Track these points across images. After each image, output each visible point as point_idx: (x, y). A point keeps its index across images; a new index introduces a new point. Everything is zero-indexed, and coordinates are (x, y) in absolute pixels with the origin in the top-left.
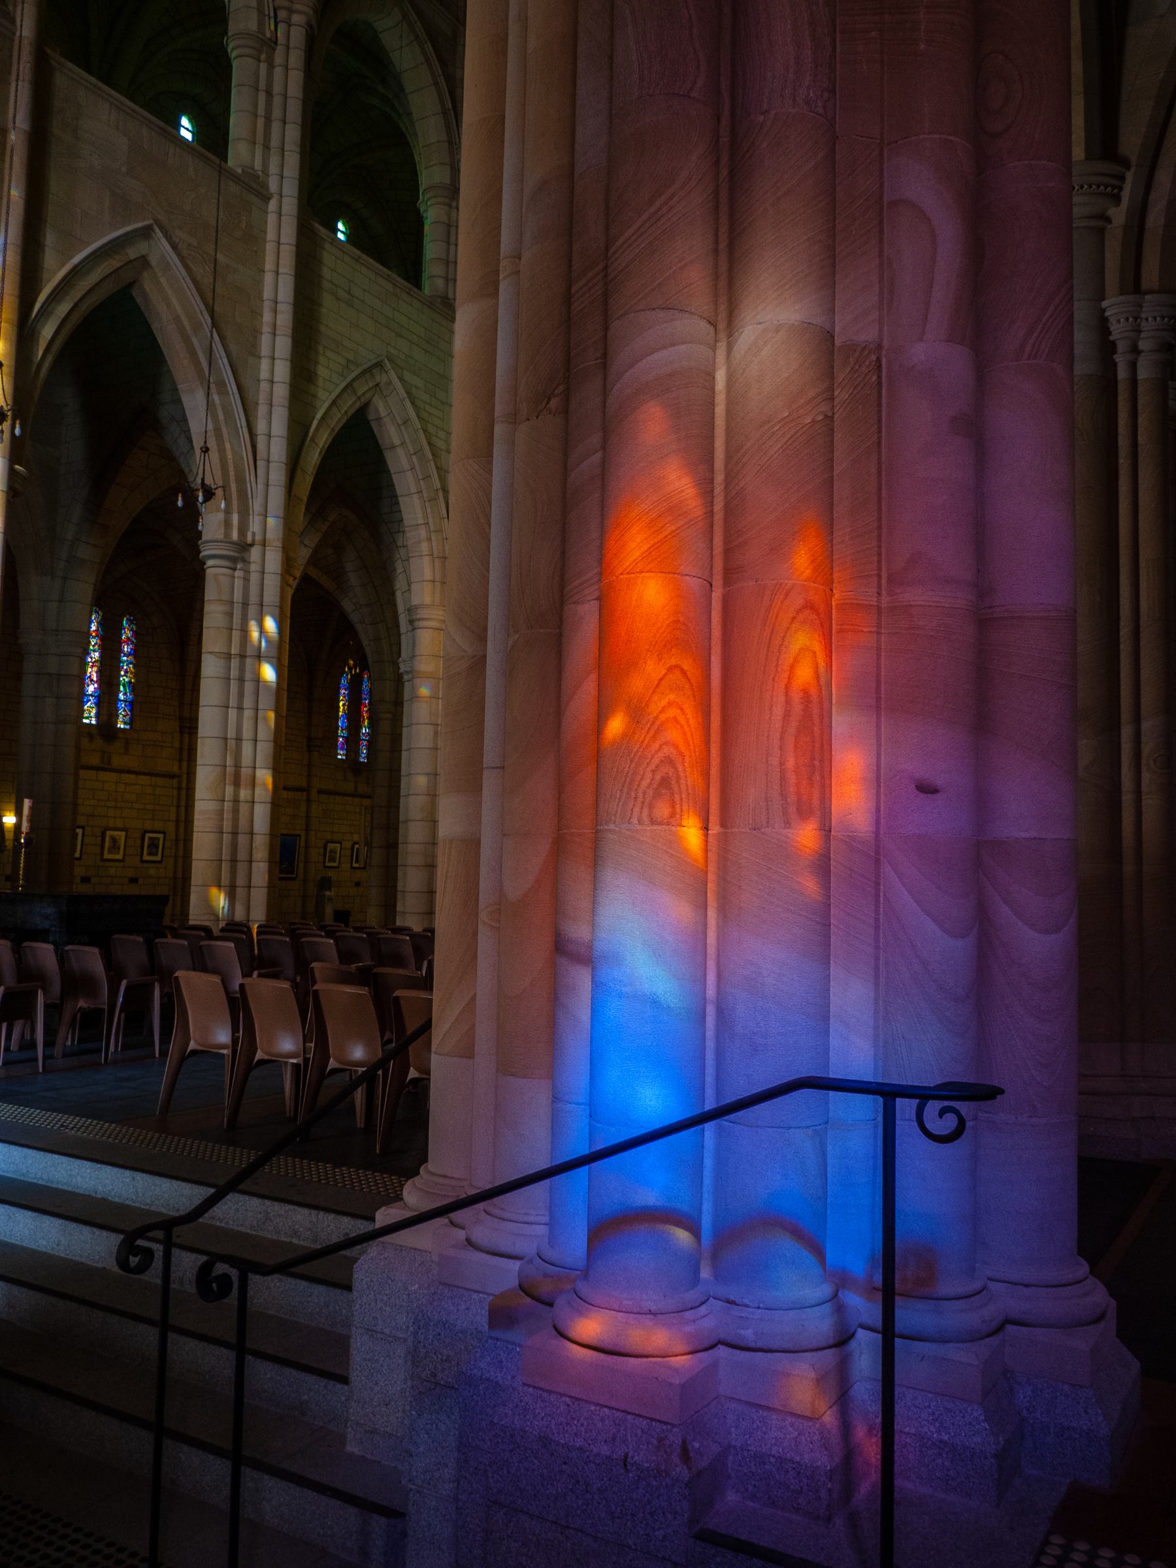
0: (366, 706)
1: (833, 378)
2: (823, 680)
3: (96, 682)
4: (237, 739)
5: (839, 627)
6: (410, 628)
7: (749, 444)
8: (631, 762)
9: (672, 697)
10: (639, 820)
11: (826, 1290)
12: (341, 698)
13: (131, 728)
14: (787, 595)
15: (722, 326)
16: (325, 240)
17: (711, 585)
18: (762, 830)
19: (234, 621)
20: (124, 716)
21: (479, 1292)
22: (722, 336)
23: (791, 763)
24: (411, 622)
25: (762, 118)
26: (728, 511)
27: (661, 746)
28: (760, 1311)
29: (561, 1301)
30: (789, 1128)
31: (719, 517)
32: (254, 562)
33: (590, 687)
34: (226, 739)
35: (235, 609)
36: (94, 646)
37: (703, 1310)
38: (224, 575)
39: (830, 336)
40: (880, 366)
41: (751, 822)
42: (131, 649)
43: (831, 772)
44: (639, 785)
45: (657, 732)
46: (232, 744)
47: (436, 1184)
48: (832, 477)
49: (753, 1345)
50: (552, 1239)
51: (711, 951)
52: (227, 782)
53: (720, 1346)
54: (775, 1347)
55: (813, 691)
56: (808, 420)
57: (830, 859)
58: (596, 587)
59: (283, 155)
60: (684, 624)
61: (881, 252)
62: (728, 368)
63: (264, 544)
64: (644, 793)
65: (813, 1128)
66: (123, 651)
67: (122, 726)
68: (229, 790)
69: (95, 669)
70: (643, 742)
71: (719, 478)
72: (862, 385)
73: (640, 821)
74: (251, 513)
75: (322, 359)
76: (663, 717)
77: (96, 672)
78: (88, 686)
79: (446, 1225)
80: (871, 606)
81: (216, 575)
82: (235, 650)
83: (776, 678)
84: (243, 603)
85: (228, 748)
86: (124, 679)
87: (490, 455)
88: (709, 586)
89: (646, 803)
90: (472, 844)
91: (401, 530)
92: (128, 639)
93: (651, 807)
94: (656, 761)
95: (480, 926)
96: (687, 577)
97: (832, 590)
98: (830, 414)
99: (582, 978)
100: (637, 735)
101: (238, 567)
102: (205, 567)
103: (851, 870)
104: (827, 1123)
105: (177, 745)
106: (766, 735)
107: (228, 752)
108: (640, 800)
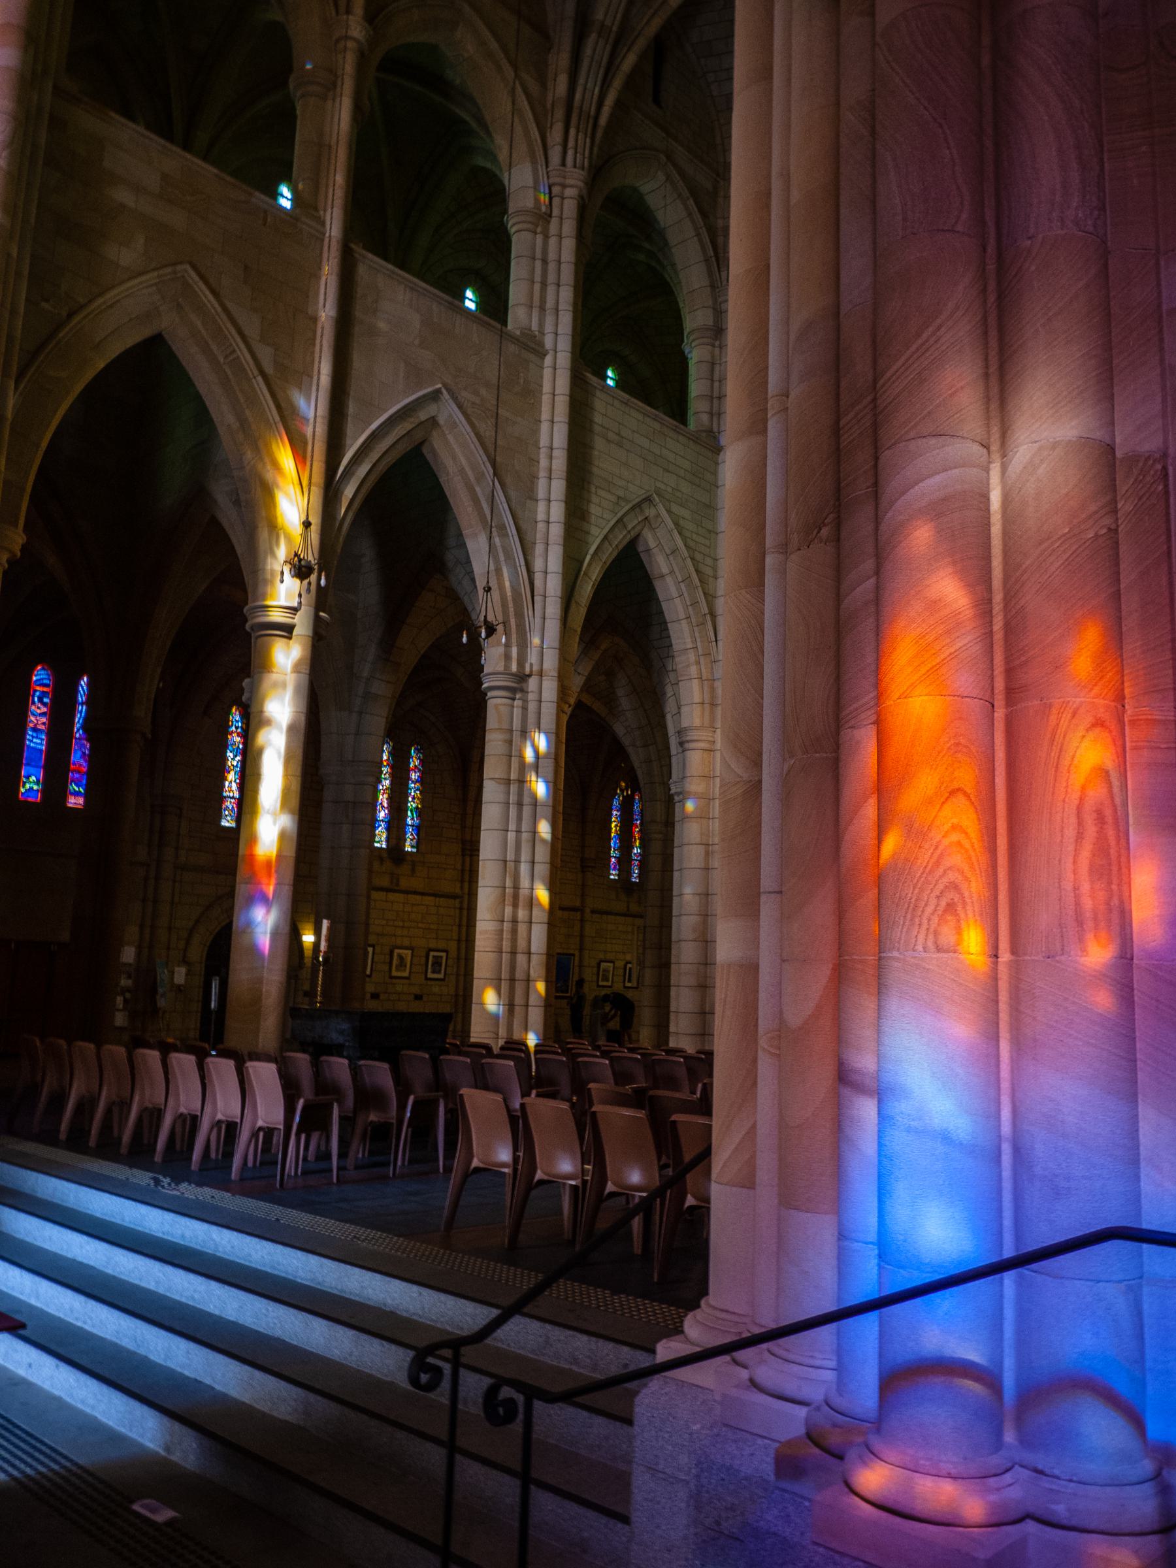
0: (637, 827)
1: (1115, 491)
2: (1118, 800)
4: (515, 861)
5: (1134, 744)
6: (680, 750)
7: (1028, 562)
8: (914, 888)
9: (955, 821)
10: (924, 948)
11: (1147, 1466)
12: (613, 819)
13: (417, 851)
14: (1074, 714)
15: (995, 447)
16: (596, 387)
17: (993, 706)
18: (1057, 958)
20: (411, 840)
21: (765, 1438)
22: (996, 456)
23: (1086, 887)
24: (681, 744)
25: (1029, 242)
26: (1008, 629)
27: (945, 871)
28: (1072, 1485)
29: (852, 1454)
30: (1099, 1282)
31: (998, 636)
32: (532, 692)
33: (870, 810)
34: (505, 861)
37: (1008, 1478)
39: (1111, 448)
40: (1166, 475)
41: (1044, 949)
43: (1130, 896)
44: (923, 911)
45: (941, 856)
46: (511, 865)
47: (718, 1318)
48: (1119, 590)
49: (1065, 1522)
50: (841, 1384)
51: (1005, 1085)
52: (506, 903)
53: (1028, 1521)
54: (1093, 1526)
55: (1108, 812)
56: (1091, 535)
57: (1132, 989)
58: (873, 711)
59: (557, 315)
60: (967, 747)
61: (1162, 360)
62: (1003, 488)
63: (541, 674)
64: (929, 920)
65: (1125, 1283)
66: (411, 779)
67: (410, 850)
68: (508, 910)
69: (386, 796)
70: (926, 867)
71: (998, 597)
72: (1147, 495)
73: (925, 949)
74: (529, 646)
75: (594, 499)
76: (946, 842)
77: (387, 799)
78: (380, 812)
79: (728, 1363)
80: (1168, 721)
81: (496, 706)
82: (513, 776)
83: (1067, 800)
86: (412, 805)
87: (762, 584)
88: (990, 705)
89: (931, 930)
90: (750, 969)
91: (670, 654)
92: (416, 766)
93: (936, 933)
94: (941, 886)
95: (760, 1053)
96: (967, 699)
97: (1123, 706)
98: (1113, 527)
99: (866, 1109)
100: (919, 861)
101: (517, 696)
102: (487, 698)
103: (1157, 1001)
104: (1141, 1277)
105: (459, 867)
106: (1057, 859)
107: (508, 875)
108: (925, 926)
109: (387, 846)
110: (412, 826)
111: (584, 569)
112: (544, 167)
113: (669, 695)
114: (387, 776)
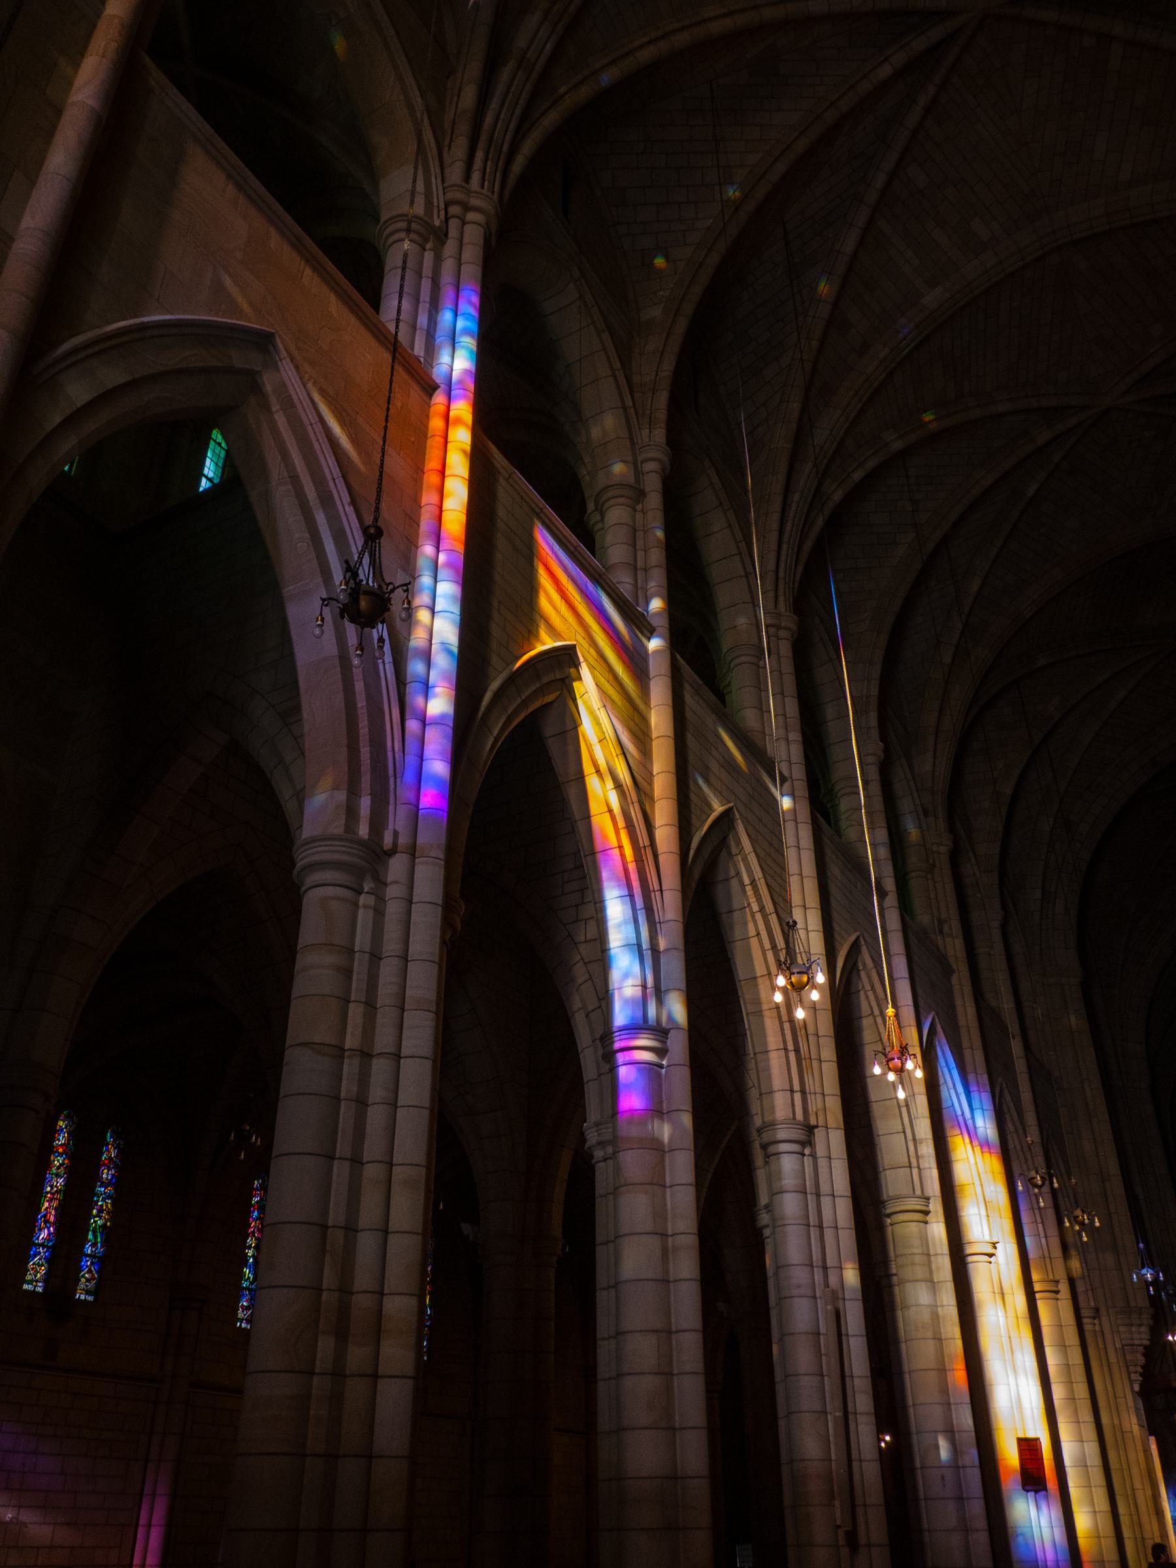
3: (53, 1224)
4: (346, 1228)
16: (499, 472)
19: (354, 986)
20: (88, 1280)
32: (396, 882)
34: (324, 1227)
35: (356, 963)
36: (58, 1168)
38: (338, 899)
42: (113, 1176)
63: (412, 851)
66: (99, 1178)
67: (83, 1297)
68: (325, 1346)
77: (56, 1209)
78: (40, 1230)
84: (371, 954)
85: (328, 1247)
92: (110, 1159)
102: (303, 889)
107: (328, 1258)
109: (45, 1288)
110: (91, 1256)
111: (480, 713)
112: (439, 179)
113: (580, 981)
114: (62, 1170)
